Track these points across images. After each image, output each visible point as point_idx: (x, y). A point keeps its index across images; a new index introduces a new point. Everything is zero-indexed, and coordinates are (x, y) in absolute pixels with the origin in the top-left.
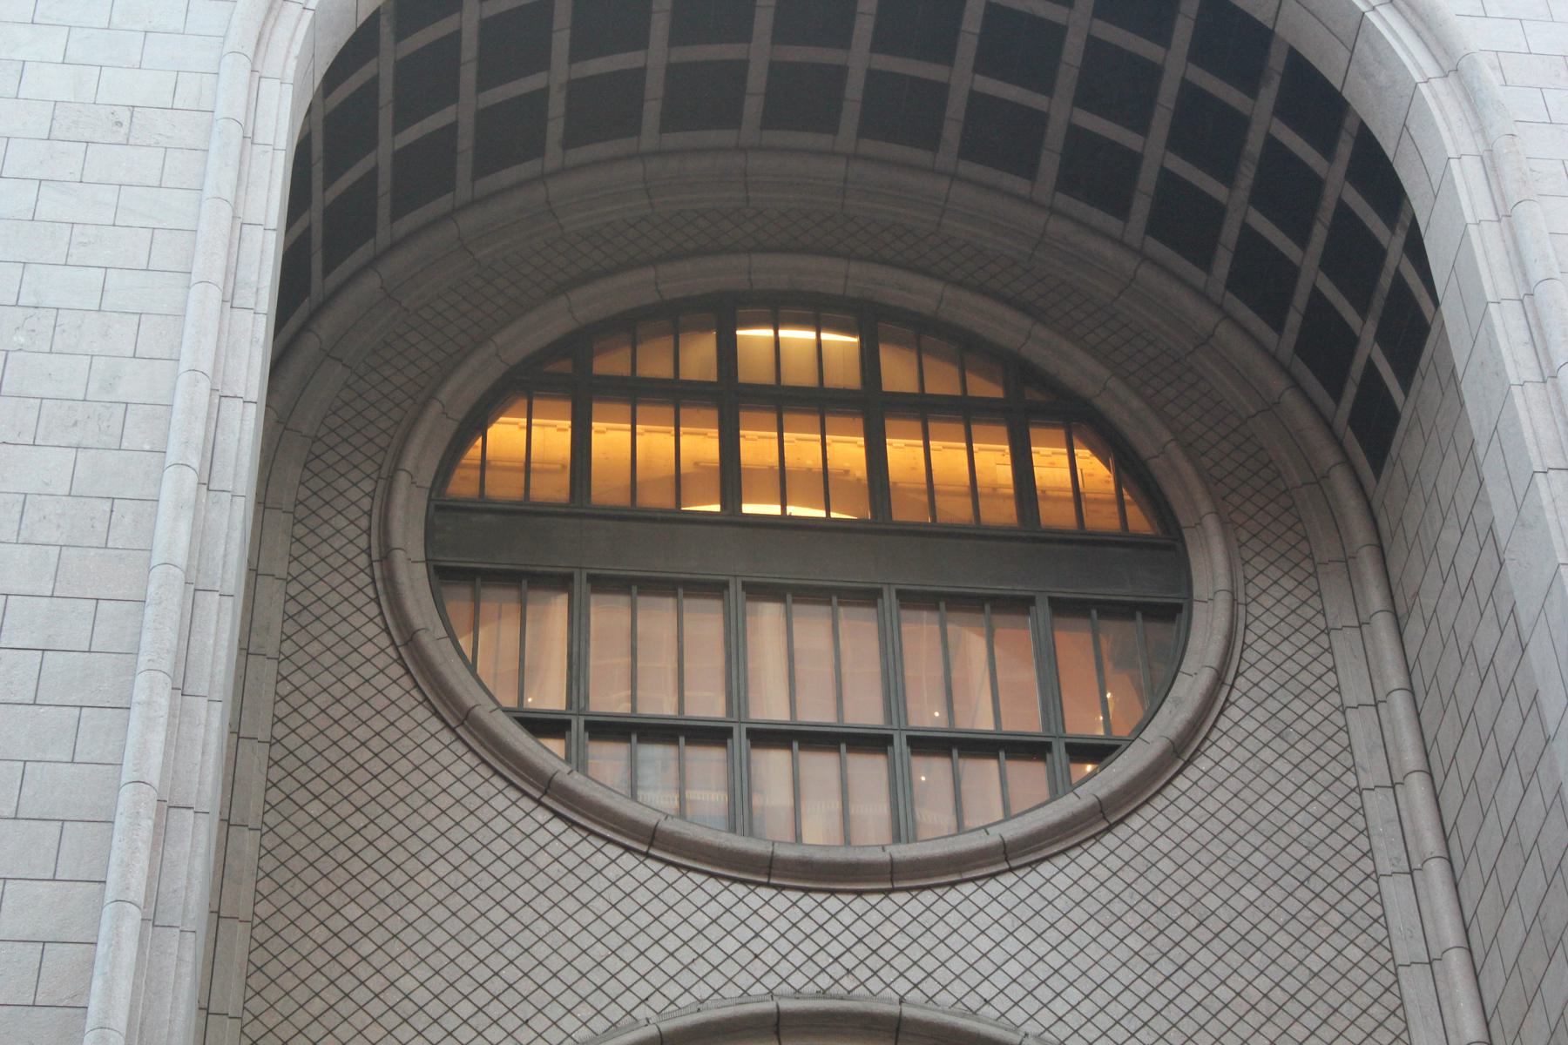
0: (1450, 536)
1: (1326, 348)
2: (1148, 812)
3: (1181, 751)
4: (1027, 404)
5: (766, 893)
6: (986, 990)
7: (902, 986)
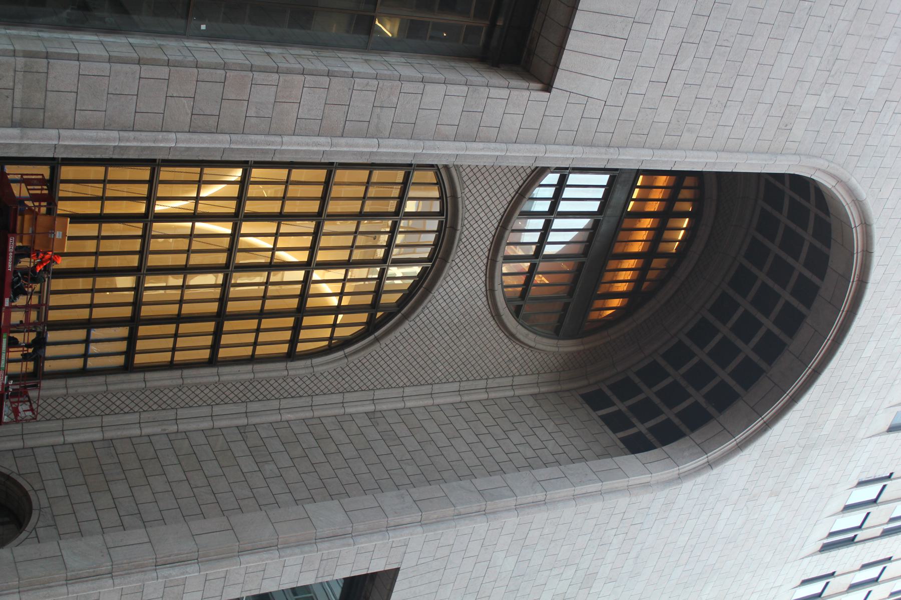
0: (551, 426)
1: (624, 388)
2: (495, 326)
3: (511, 336)
4: (636, 297)
5: (496, 225)
6: (451, 282)
7: (457, 260)
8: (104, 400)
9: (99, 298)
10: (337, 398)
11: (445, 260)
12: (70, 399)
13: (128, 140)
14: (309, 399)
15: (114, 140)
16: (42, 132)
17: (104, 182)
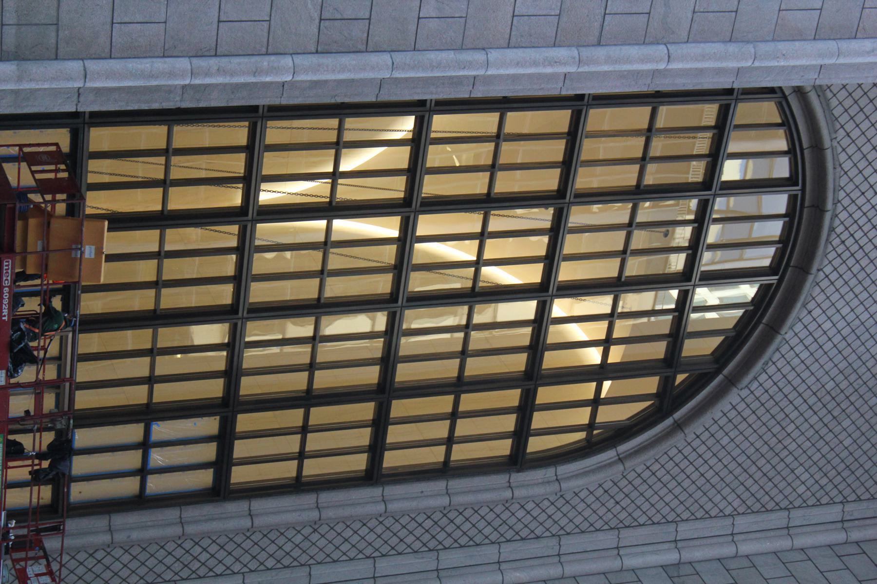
6: (817, 312)
7: (828, 270)
8: (179, 552)
9: (165, 365)
10: (607, 539)
11: (804, 269)
12: (117, 553)
13: (207, 74)
14: (554, 542)
15: (183, 76)
16: (54, 67)
17: (167, 152)
